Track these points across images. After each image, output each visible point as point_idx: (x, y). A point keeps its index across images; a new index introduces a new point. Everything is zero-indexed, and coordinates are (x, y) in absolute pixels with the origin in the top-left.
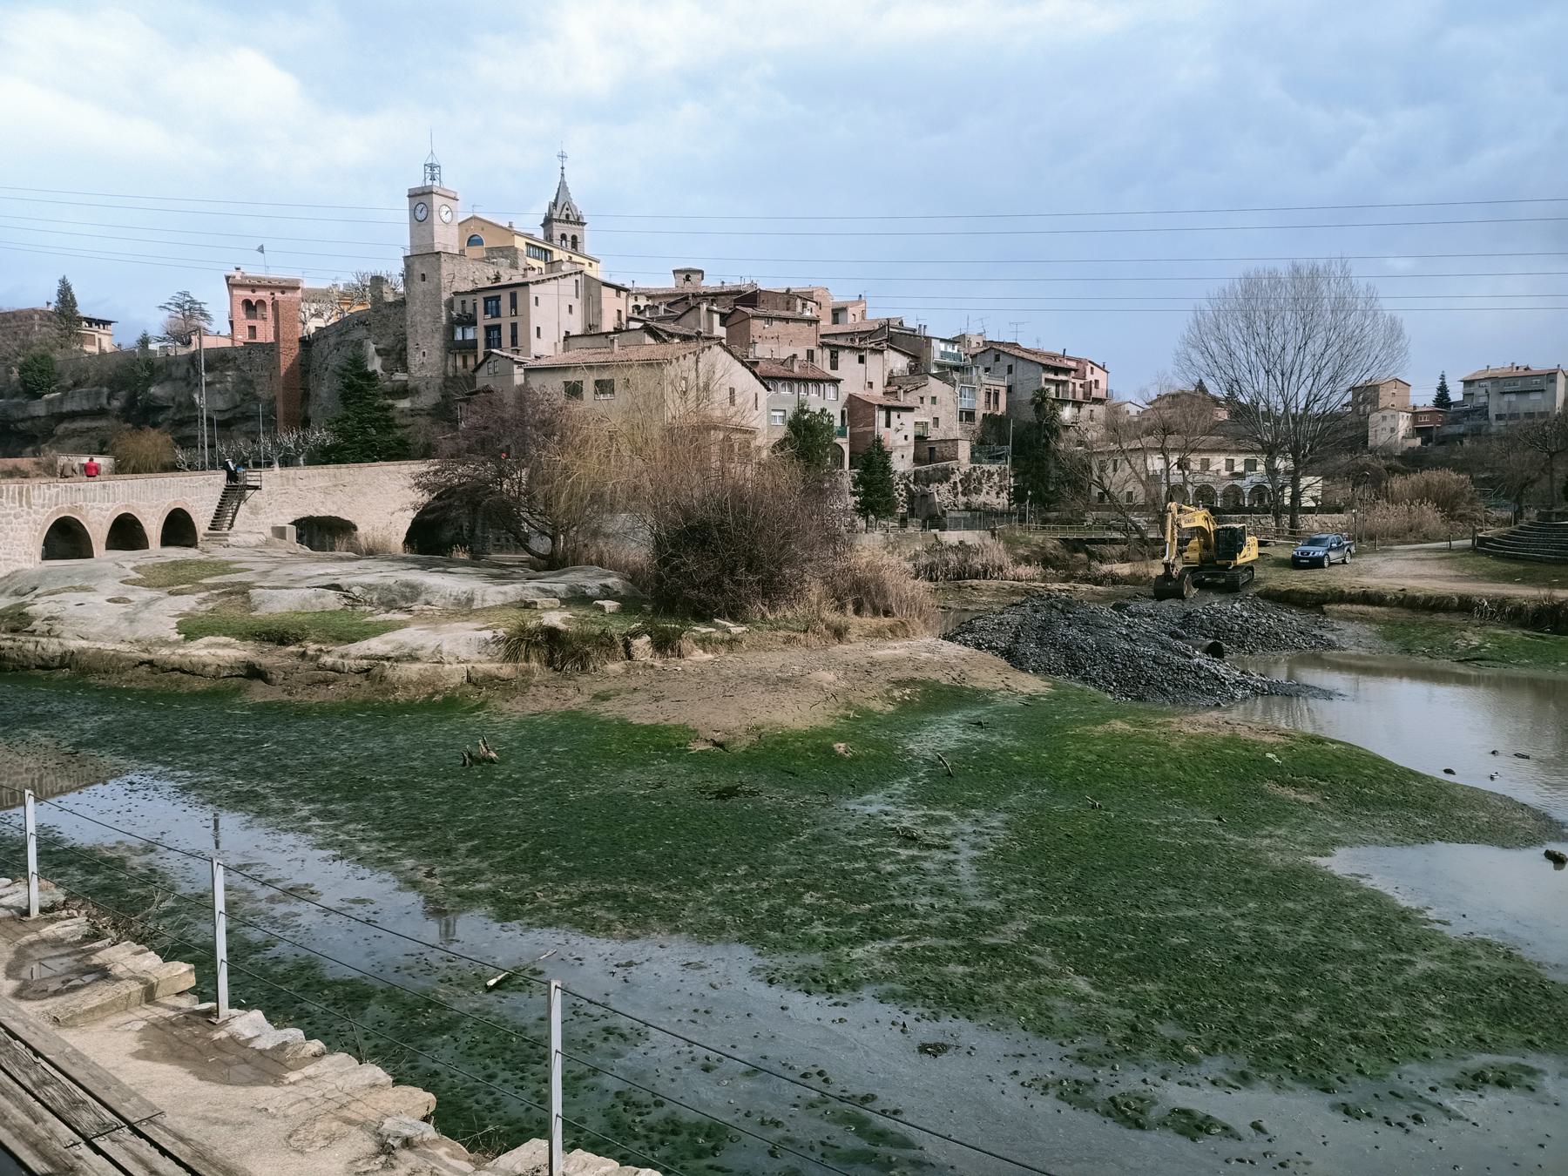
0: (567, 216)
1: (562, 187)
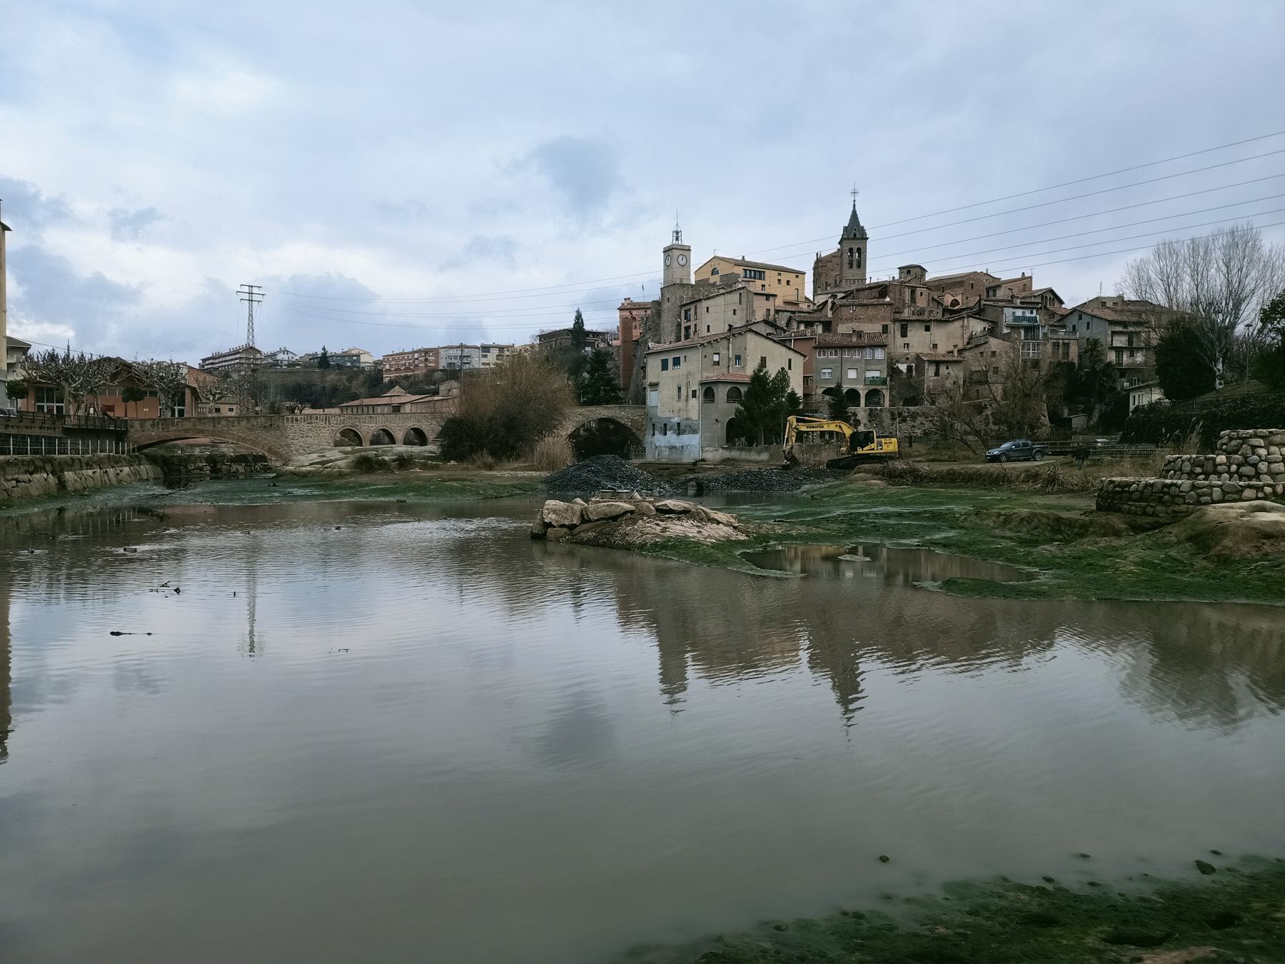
0: (855, 235)
1: (854, 215)
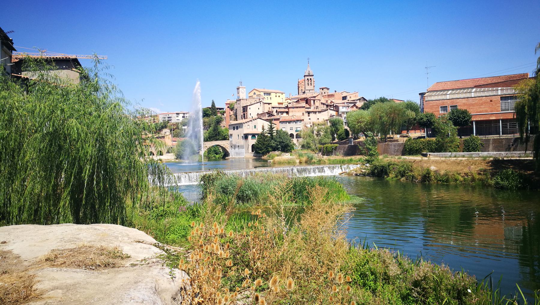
0: (309, 74)
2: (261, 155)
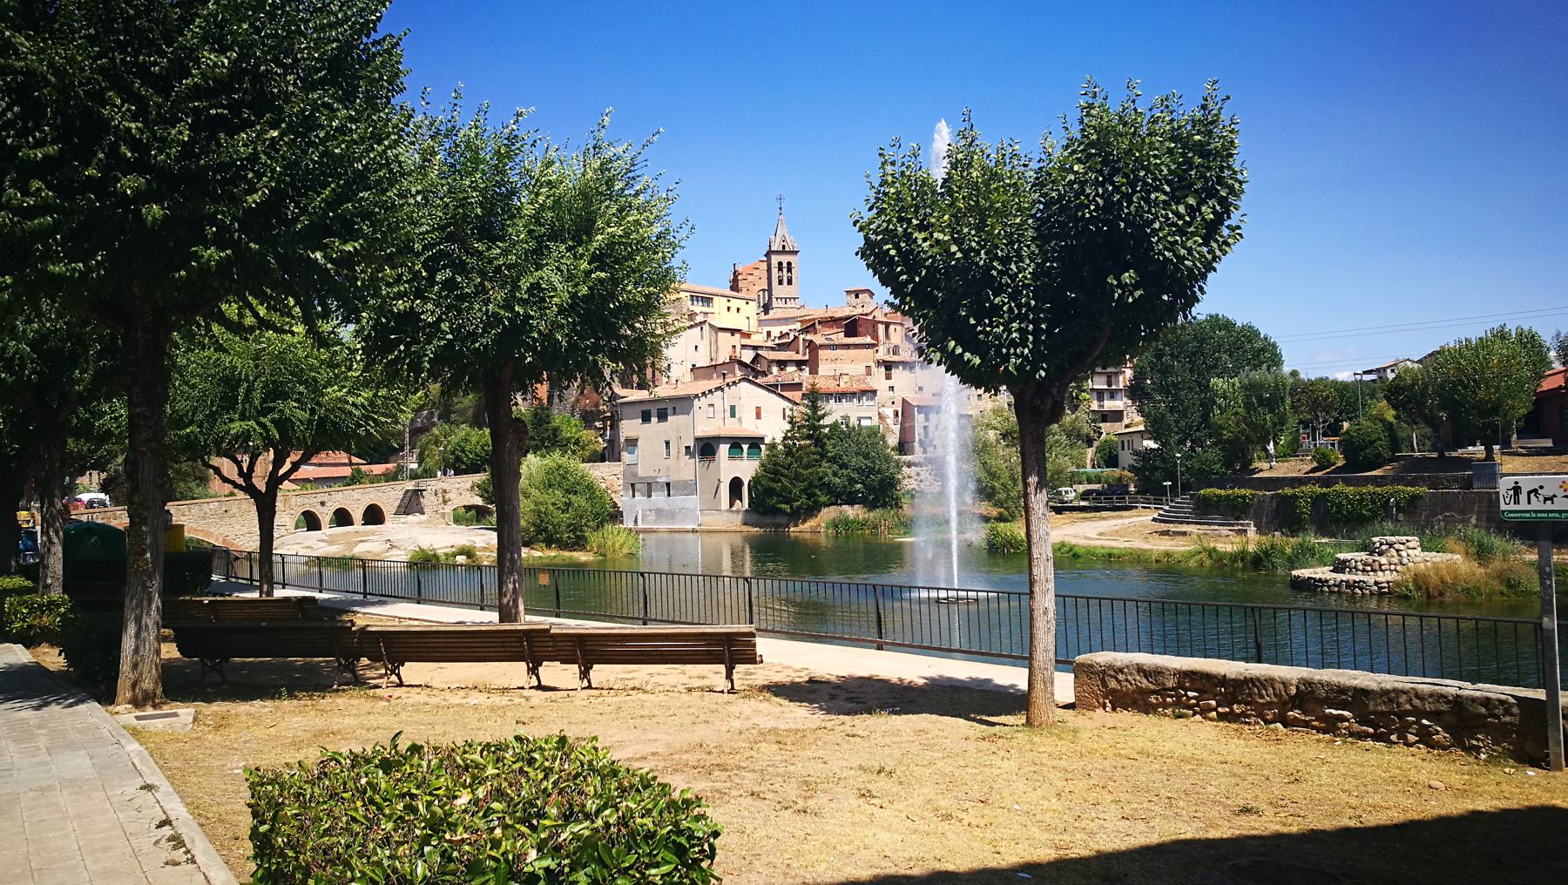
0: (784, 247)
2: (781, 520)
